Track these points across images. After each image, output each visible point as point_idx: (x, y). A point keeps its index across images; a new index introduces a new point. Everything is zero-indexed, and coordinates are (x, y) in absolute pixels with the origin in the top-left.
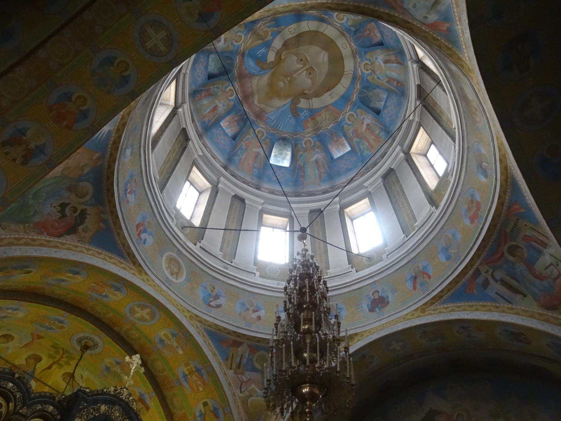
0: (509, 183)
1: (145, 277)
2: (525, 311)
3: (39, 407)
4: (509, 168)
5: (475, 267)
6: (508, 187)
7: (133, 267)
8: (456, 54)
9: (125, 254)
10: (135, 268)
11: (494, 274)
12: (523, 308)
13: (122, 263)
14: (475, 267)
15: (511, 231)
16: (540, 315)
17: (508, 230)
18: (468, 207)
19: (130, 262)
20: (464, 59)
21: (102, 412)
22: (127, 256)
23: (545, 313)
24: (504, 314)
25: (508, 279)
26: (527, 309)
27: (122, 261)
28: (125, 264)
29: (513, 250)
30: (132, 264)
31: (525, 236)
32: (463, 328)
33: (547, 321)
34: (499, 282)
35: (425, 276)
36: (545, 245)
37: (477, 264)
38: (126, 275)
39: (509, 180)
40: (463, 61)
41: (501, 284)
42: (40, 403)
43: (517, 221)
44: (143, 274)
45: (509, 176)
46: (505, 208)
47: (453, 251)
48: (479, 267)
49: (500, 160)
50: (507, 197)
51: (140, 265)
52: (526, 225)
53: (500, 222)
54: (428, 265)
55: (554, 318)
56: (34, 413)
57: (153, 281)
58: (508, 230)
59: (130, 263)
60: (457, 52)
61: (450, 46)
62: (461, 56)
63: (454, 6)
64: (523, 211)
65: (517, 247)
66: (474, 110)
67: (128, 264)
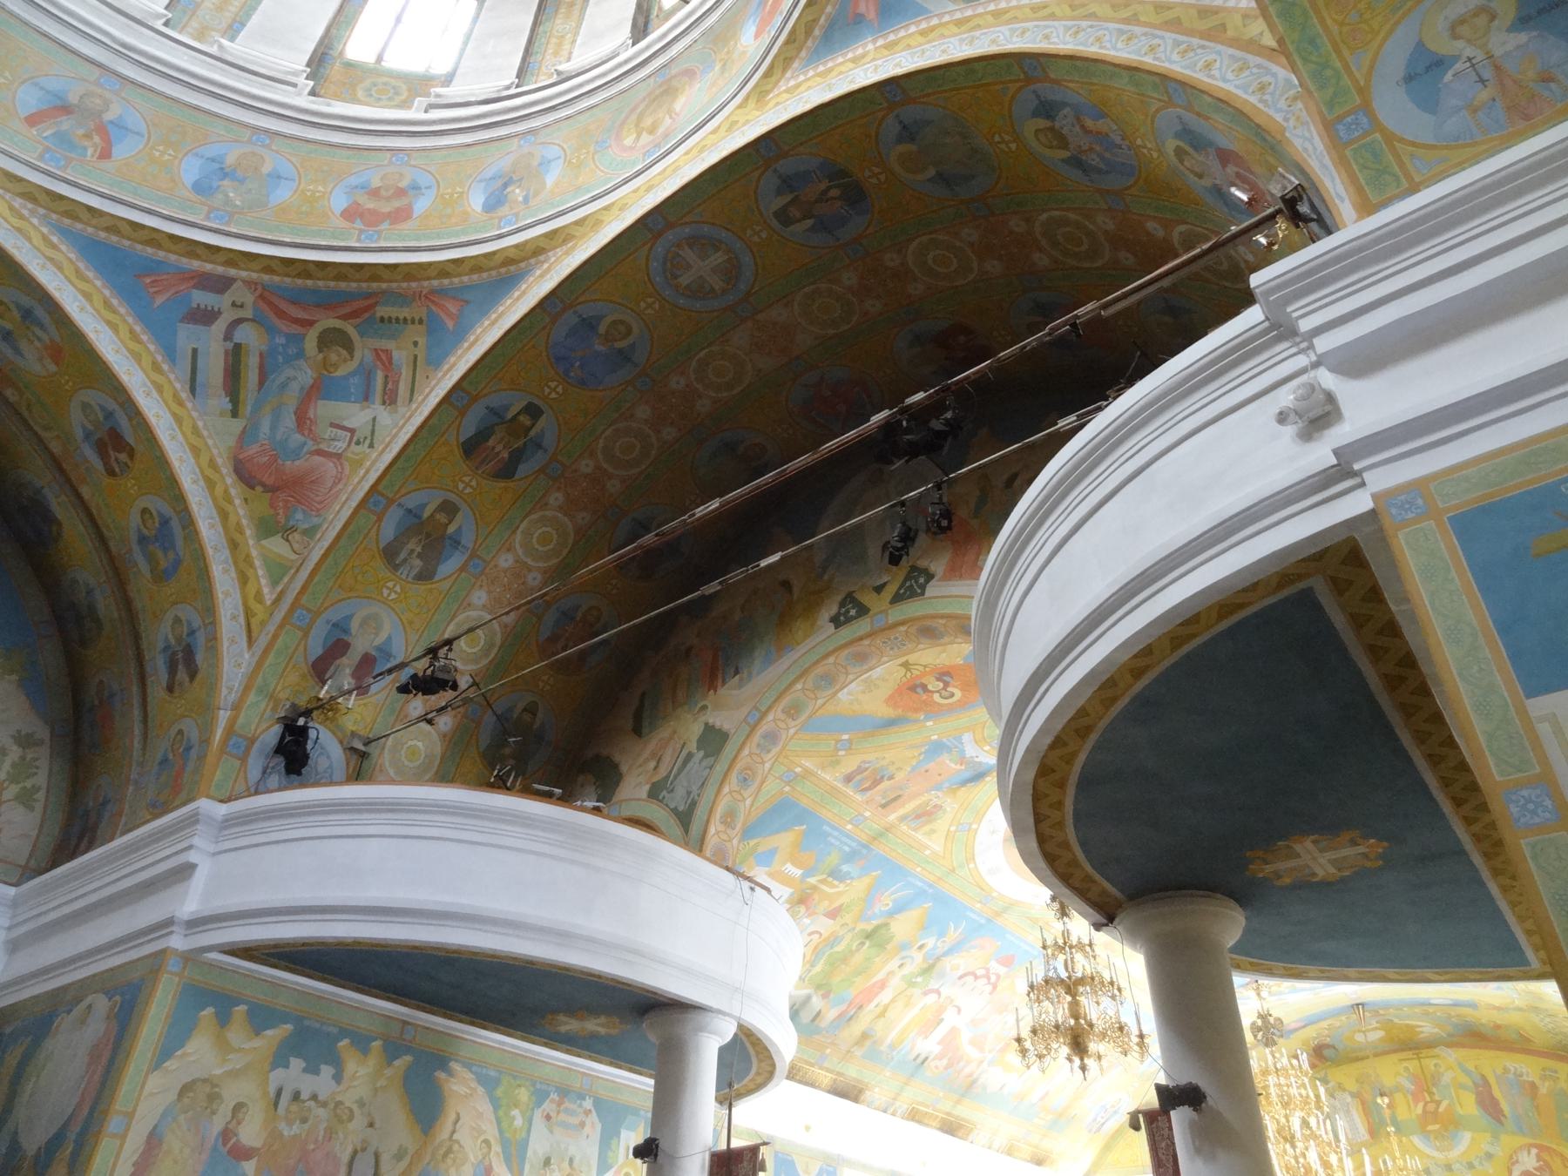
0: (503, 270)
2: (196, 431)
4: (542, 258)
5: (232, 272)
6: (494, 273)
8: (800, 50)
11: (244, 325)
12: (200, 424)
14: (232, 272)
15: (382, 320)
16: (212, 464)
17: (382, 311)
18: (379, 188)
20: (788, 74)
23: (224, 471)
24: (155, 394)
26: (205, 433)
29: (329, 339)
31: (388, 353)
32: (27, 314)
33: (210, 484)
34: (230, 345)
35: (97, 139)
36: (390, 399)
37: (244, 274)
39: (512, 268)
40: (784, 71)
41: (226, 352)
43: (417, 322)
45: (523, 265)
46: (435, 283)
47: (231, 195)
48: (239, 283)
49: (555, 232)
50: (465, 279)
52: (416, 344)
53: (394, 285)
54: (138, 133)
55: (226, 491)
58: (382, 311)
60: (803, 54)
61: (817, 32)
62: (796, 65)
63: (924, 25)
64: (450, 324)
65: (348, 346)
66: (648, 122)
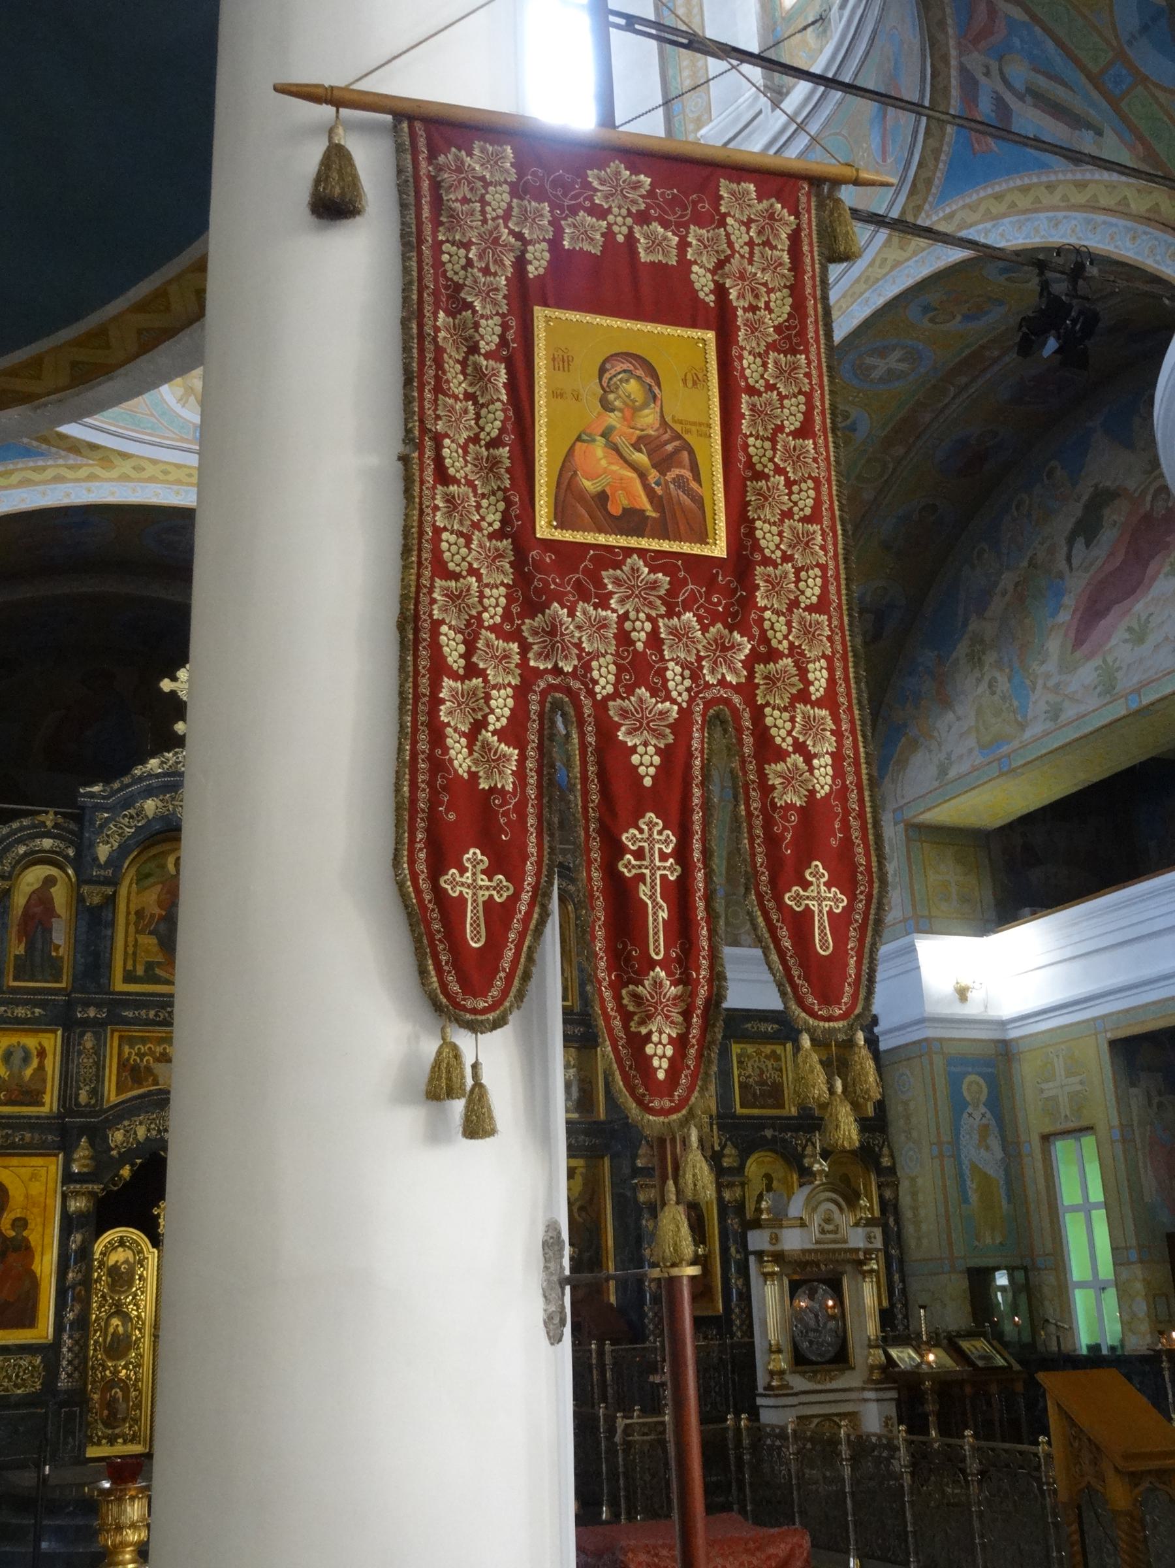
1: (126, 467)
3: (22, 850)
7: (80, 460)
9: (35, 443)
10: (85, 461)
11: (1007, 70)
13: (44, 469)
19: (63, 453)
21: (150, 815)
22: (44, 446)
25: (1042, 82)
27: (41, 463)
28: (51, 466)
30: (72, 456)
34: (1028, 98)
38: (68, 495)
41: (1035, 106)
42: (20, 841)
44: (117, 461)
51: (94, 447)
56: (18, 862)
57: (154, 462)
59: (64, 457)
67: (61, 462)
